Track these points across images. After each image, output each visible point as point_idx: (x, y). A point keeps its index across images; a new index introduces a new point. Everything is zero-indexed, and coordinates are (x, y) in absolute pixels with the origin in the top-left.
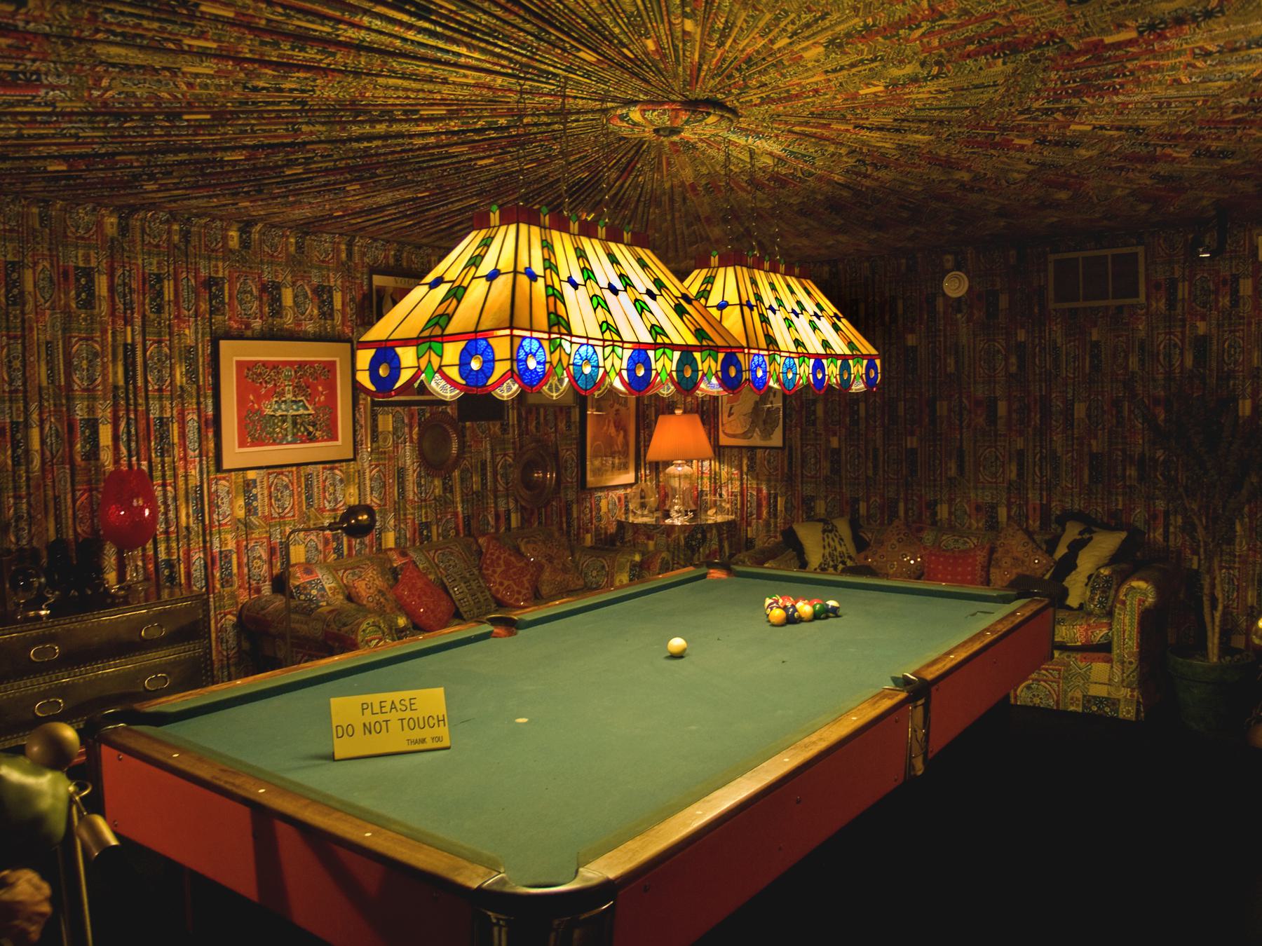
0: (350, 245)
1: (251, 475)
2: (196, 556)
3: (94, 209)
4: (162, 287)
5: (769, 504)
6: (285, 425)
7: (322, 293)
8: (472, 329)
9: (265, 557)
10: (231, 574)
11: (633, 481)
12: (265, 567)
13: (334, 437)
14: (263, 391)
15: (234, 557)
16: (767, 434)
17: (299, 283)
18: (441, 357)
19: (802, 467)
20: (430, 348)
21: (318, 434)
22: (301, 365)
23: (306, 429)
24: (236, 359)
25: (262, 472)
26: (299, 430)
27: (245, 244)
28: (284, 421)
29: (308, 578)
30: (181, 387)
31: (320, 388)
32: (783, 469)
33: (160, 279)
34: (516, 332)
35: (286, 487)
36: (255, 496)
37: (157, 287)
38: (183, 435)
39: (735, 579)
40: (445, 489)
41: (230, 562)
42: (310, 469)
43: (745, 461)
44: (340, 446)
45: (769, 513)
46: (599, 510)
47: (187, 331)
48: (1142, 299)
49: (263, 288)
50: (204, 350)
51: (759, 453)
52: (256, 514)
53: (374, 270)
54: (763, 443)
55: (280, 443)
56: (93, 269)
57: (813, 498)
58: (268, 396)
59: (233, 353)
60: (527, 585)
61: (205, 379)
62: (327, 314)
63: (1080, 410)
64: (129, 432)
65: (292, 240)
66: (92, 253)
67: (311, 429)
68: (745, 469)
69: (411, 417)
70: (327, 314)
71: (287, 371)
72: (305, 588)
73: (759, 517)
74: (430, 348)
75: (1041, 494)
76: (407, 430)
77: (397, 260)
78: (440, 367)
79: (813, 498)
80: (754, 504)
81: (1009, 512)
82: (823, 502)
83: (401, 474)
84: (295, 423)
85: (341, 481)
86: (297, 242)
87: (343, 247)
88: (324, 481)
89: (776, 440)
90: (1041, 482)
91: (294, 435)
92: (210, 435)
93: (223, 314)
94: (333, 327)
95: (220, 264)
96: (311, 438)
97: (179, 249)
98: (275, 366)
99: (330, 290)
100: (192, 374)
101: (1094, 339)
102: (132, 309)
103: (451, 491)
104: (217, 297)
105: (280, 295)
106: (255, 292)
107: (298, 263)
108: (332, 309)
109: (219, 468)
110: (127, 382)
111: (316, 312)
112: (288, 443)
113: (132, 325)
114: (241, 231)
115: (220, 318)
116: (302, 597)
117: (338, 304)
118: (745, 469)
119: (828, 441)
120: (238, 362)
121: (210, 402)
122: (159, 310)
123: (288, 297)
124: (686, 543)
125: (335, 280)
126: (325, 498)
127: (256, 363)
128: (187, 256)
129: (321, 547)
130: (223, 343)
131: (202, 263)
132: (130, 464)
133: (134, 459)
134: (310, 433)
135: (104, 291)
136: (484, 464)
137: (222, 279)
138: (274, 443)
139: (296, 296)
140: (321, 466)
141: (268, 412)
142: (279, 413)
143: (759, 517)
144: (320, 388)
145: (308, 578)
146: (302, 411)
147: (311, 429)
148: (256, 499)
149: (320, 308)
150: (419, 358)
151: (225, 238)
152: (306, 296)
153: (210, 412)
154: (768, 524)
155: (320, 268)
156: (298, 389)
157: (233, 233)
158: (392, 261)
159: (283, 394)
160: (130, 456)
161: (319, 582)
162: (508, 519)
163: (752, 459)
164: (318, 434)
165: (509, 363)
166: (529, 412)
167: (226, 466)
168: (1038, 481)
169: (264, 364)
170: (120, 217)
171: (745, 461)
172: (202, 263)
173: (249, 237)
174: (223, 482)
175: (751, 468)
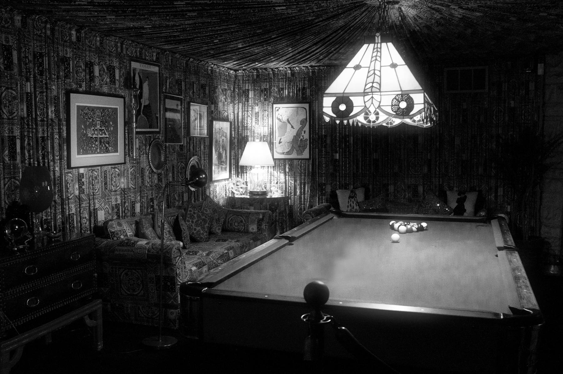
0: (122, 44)
1: (82, 171)
2: (58, 217)
3: (11, 10)
4: (43, 61)
5: (301, 188)
6: (97, 143)
7: (111, 69)
8: (342, 92)
9: (87, 218)
10: (74, 227)
11: (228, 177)
12: (88, 223)
13: (116, 151)
14: (88, 123)
15: (75, 217)
16: (300, 152)
17: (101, 63)
18: (380, 102)
19: (319, 169)
20: (372, 97)
21: (110, 148)
22: (104, 109)
23: (105, 146)
24: (77, 104)
25: (86, 169)
26: (102, 146)
27: (78, 39)
28: (96, 141)
29: (119, 228)
30: (52, 119)
31: (111, 123)
32: (308, 168)
33: (41, 56)
34: (382, 93)
35: (96, 178)
36: (83, 183)
37: (40, 60)
38: (53, 147)
39: (343, 220)
40: (159, 180)
41: (73, 220)
42: (105, 168)
43: (287, 166)
44: (116, 157)
45: (301, 192)
46: (216, 192)
47: (54, 87)
48: (487, 89)
49: (86, 65)
50: (62, 99)
51: (295, 162)
52: (84, 193)
53: (133, 59)
54: (300, 157)
55: (94, 153)
56: (11, 46)
57: (325, 184)
58: (90, 126)
59: (78, 101)
60: (206, 230)
61: (63, 116)
62: (113, 81)
63: (457, 141)
64: (29, 144)
65: (98, 39)
66: (10, 36)
67: (107, 145)
68: (287, 170)
69: (146, 140)
70: (113, 81)
71: (98, 113)
72: (117, 234)
73: (295, 194)
74: (372, 97)
75: (439, 180)
76: (144, 147)
77: (140, 54)
78: (379, 106)
79: (325, 184)
80: (293, 188)
81: (424, 188)
82: (329, 186)
83: (143, 169)
84: (101, 142)
85: (119, 175)
86: (100, 40)
87: (119, 45)
88: (112, 175)
89: (306, 154)
90: (439, 174)
91: (100, 148)
92: (65, 147)
93: (70, 78)
94: (115, 89)
95: (68, 50)
96: (107, 151)
97: (50, 39)
98: (93, 109)
99: (114, 69)
100: (57, 112)
101: (465, 107)
102: (30, 72)
103: (161, 181)
104: (67, 68)
105: (93, 69)
106: (83, 67)
107: (100, 51)
108: (115, 79)
109: (69, 167)
110: (28, 115)
111: (108, 80)
112: (98, 153)
113: (30, 82)
114: (78, 31)
115: (68, 80)
116: (115, 238)
117: (117, 77)
118: (287, 170)
119: (333, 156)
120: (78, 106)
121: (65, 128)
122: (41, 73)
123: (96, 69)
124: (270, 207)
125: (116, 64)
126: (112, 184)
127: (86, 106)
128: (53, 43)
129: (110, 212)
130: (72, 95)
131: (60, 48)
132: (30, 164)
133: (32, 160)
134: (107, 148)
135: (15, 61)
136: (173, 167)
137: (69, 58)
138: (92, 153)
139: (100, 71)
140: (110, 167)
141: (90, 135)
142: (94, 136)
143: (295, 194)
144: (111, 123)
145: (119, 228)
146: (103, 136)
147: (107, 145)
148: (84, 185)
149: (110, 78)
150: (365, 102)
151: (70, 35)
152: (104, 71)
153: (65, 135)
154: (300, 198)
155: (110, 55)
156: (103, 123)
157: (74, 32)
158: (138, 54)
159: (95, 126)
160: (30, 159)
161: (124, 231)
162: (183, 196)
163: (291, 166)
164: (110, 148)
165: (423, 105)
166: (190, 140)
167: (73, 165)
168: (437, 173)
169: (89, 108)
170: (22, 17)
171: (287, 166)
172: (60, 48)
173: (80, 35)
174: (70, 174)
175: (290, 169)
